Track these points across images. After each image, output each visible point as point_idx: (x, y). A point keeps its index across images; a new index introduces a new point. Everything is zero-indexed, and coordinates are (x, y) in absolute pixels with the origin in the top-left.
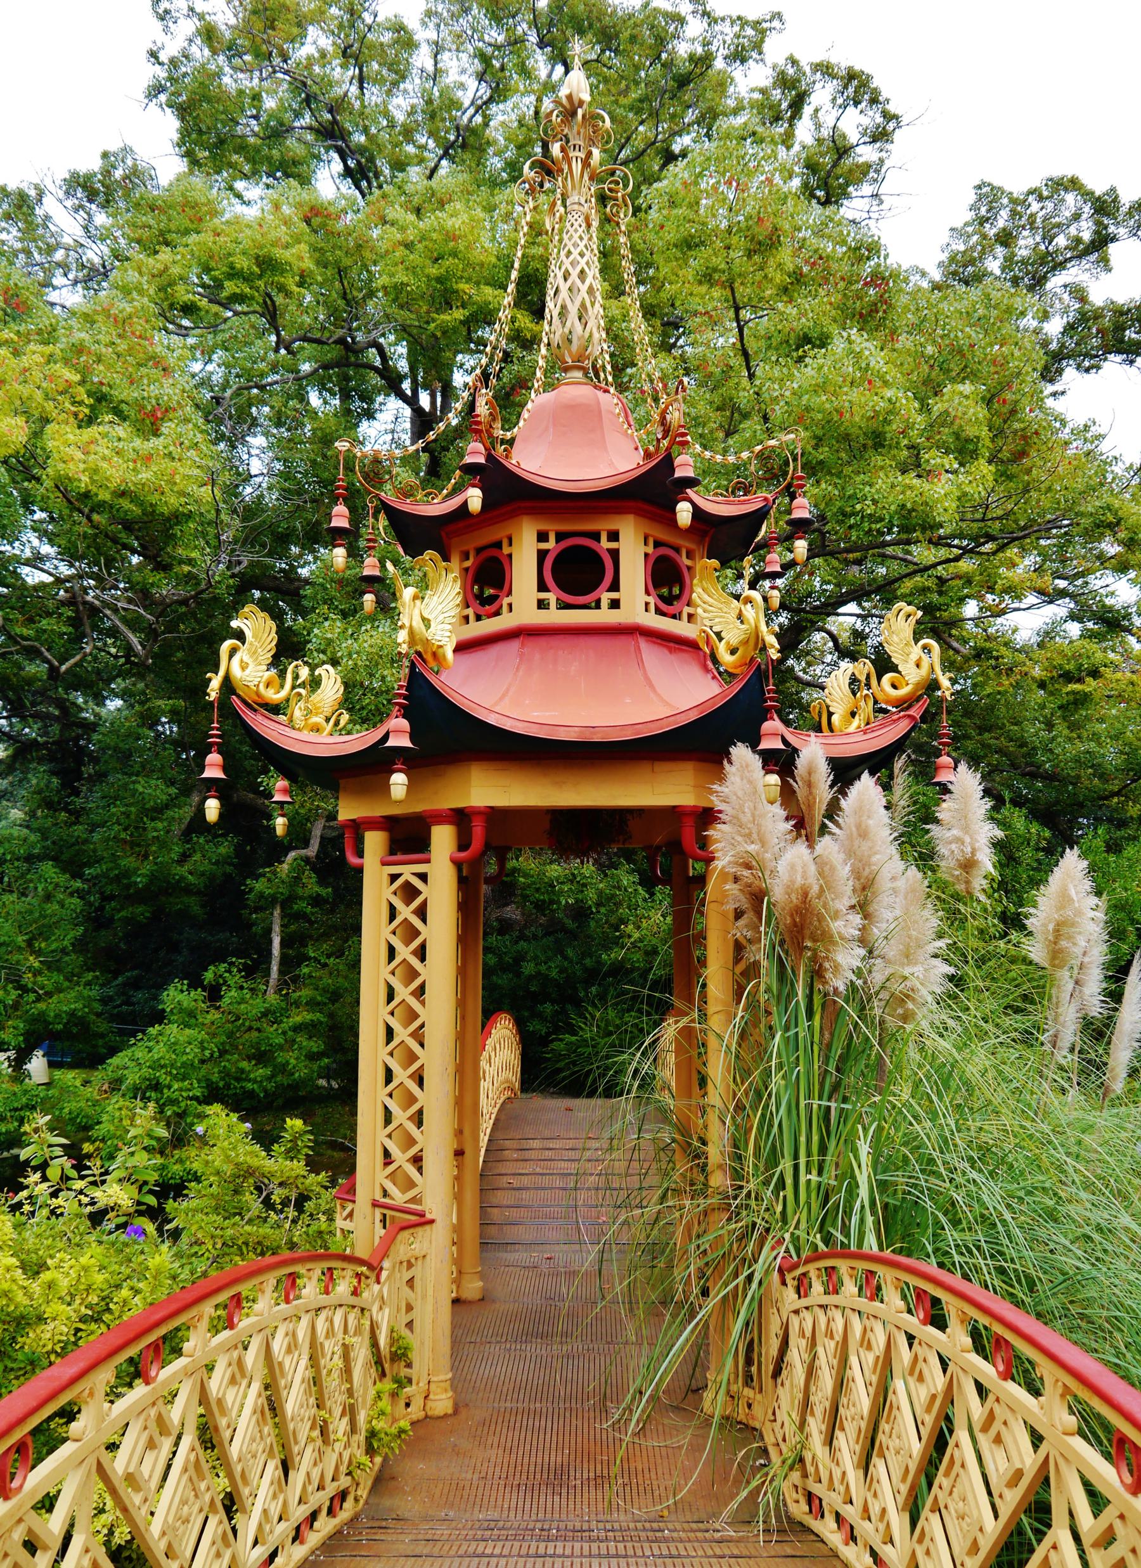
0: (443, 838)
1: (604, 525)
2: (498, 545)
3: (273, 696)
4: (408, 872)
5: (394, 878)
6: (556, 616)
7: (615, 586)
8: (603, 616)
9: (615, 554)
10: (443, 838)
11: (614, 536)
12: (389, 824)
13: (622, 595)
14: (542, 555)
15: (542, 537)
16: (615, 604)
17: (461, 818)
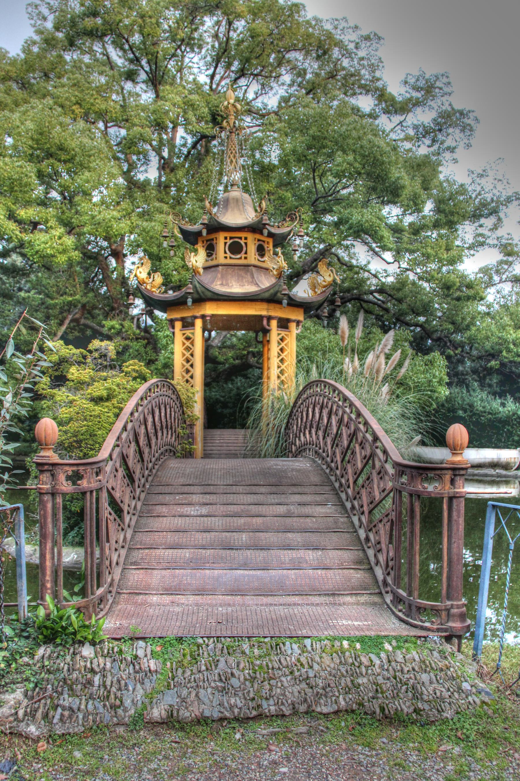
0: (199, 323)
1: (243, 235)
2: (213, 240)
3: (147, 281)
4: (188, 333)
5: (184, 334)
6: (229, 261)
7: (246, 253)
8: (243, 262)
9: (246, 244)
10: (199, 323)
11: (246, 238)
12: (182, 319)
13: (248, 256)
14: (225, 243)
15: (226, 238)
16: (246, 258)
17: (203, 317)
